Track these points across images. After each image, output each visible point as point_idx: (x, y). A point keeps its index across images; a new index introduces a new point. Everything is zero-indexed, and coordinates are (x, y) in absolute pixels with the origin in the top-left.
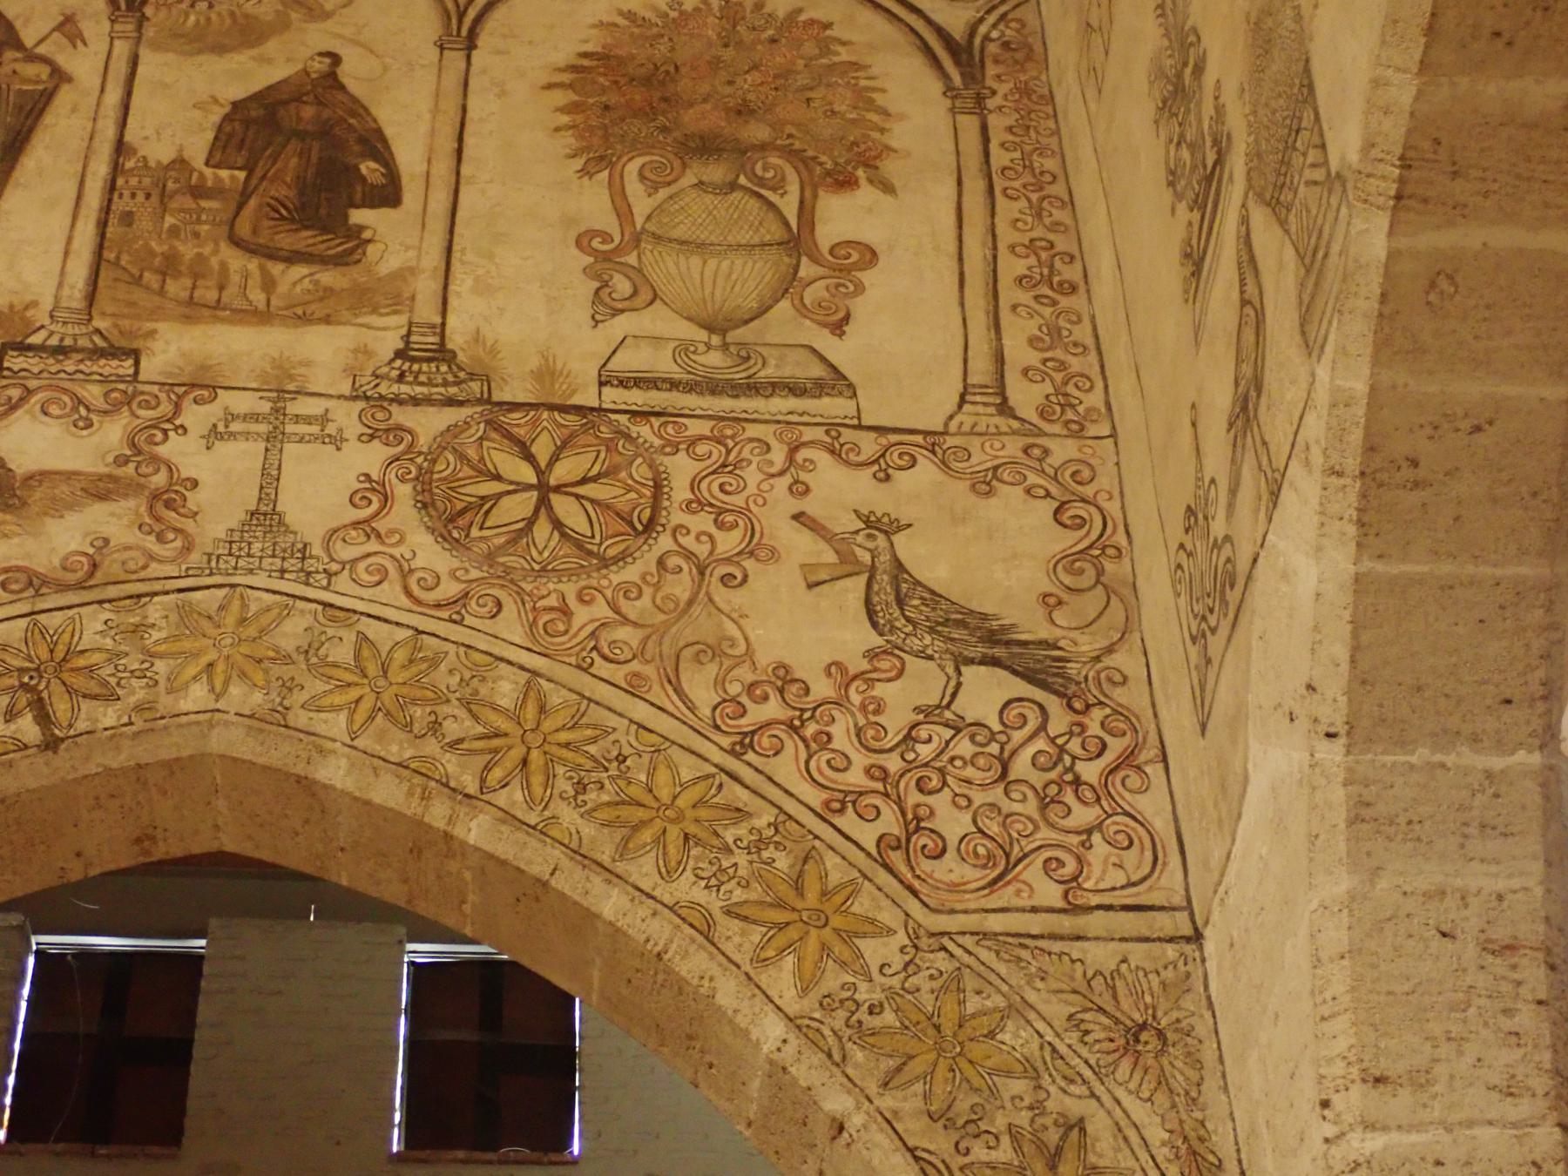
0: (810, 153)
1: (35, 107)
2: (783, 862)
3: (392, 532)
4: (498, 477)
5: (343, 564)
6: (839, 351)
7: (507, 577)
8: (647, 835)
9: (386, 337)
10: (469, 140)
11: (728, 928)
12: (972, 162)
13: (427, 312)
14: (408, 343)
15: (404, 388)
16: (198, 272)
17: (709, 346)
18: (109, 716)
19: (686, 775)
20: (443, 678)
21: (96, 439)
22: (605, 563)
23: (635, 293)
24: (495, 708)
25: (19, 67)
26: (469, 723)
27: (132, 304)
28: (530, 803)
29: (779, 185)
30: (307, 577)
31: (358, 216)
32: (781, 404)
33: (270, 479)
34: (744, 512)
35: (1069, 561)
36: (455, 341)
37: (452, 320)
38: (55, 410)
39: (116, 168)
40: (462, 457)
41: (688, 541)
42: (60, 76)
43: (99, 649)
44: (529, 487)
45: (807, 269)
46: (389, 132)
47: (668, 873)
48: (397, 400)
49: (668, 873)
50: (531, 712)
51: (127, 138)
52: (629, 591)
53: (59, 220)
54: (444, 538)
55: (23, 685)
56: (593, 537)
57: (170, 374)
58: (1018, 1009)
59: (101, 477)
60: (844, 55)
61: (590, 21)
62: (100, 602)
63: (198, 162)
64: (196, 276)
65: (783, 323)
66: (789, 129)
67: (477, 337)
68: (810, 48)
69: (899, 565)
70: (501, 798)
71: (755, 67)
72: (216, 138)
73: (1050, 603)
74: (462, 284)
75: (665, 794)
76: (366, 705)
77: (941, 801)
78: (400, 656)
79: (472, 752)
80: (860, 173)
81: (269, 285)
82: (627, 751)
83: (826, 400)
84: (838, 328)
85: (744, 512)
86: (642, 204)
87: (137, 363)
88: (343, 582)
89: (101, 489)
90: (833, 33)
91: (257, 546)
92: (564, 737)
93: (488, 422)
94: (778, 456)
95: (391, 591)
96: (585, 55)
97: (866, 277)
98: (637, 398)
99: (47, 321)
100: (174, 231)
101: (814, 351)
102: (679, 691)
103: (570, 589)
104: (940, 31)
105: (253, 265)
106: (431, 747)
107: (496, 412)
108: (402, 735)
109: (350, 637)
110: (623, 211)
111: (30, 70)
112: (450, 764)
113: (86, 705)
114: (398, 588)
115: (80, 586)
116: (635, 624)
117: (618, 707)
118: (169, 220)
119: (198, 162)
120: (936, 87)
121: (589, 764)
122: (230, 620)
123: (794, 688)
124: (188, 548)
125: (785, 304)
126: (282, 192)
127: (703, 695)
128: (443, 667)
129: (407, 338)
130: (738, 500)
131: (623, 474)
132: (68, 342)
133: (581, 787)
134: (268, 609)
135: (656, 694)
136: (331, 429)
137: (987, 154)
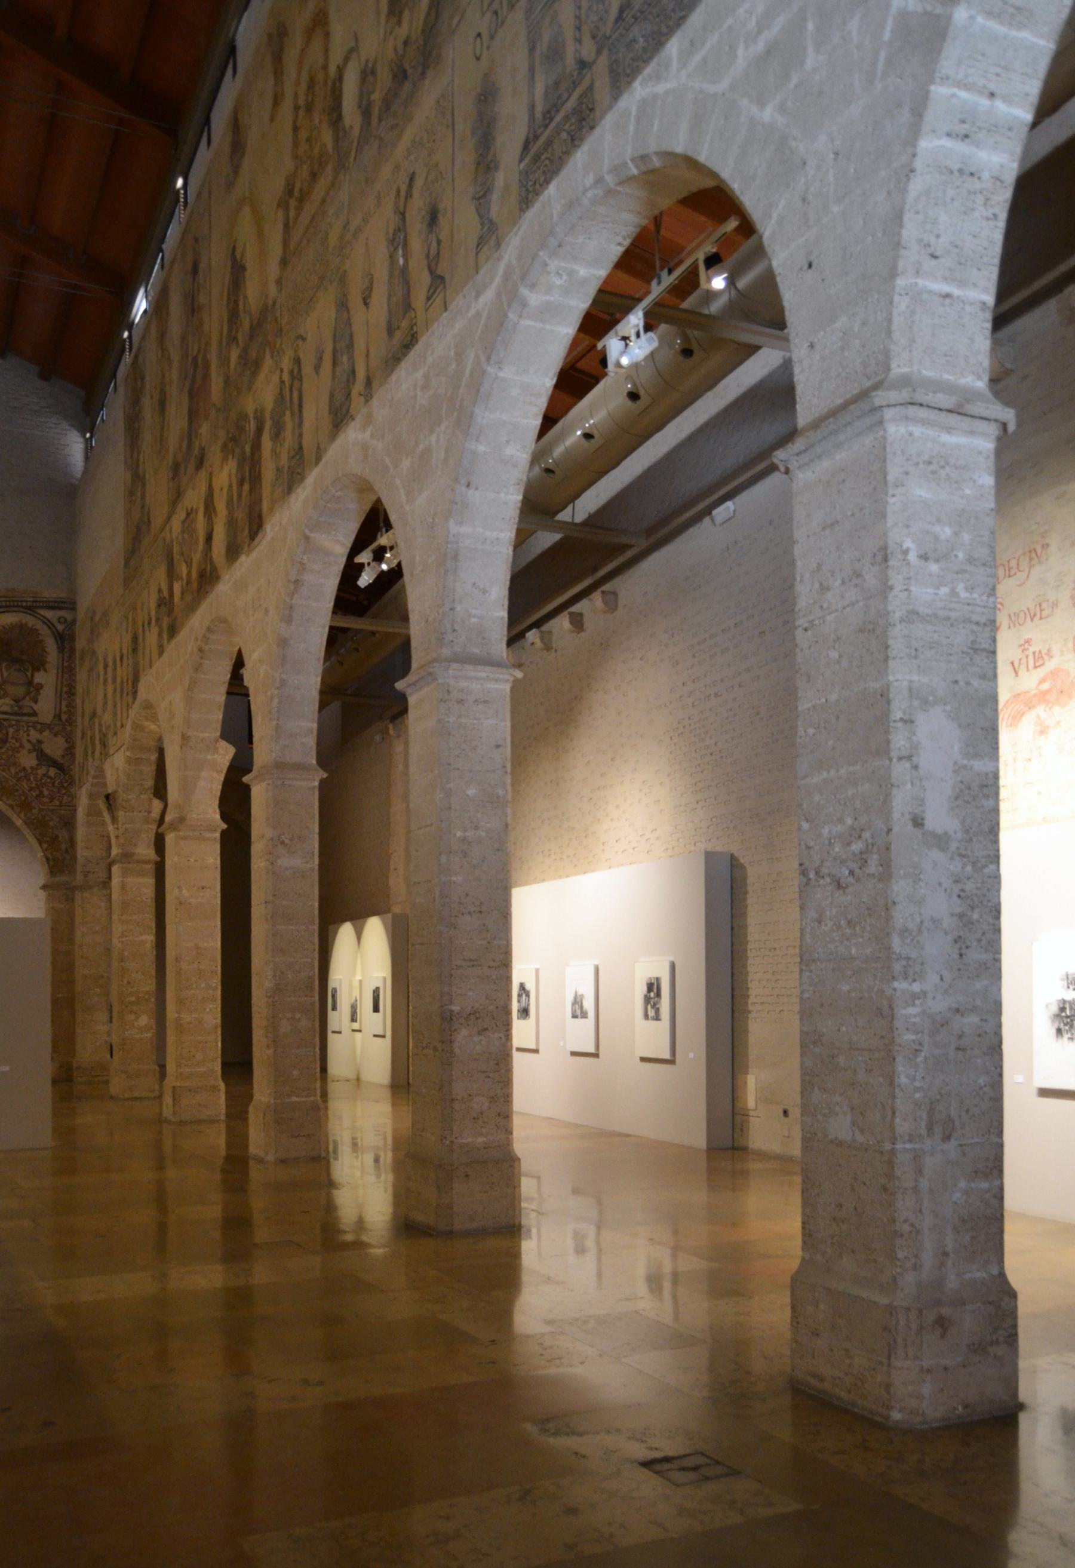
2: (23, 798)
6: (36, 707)
11: (15, 808)
19: (11, 784)
32: (26, 718)
35: (66, 750)
45: (32, 689)
47: (8, 799)
49: (8, 799)
58: (52, 820)
65: (27, 702)
69: (42, 751)
73: (63, 756)
77: (45, 789)
84: (36, 702)
97: (41, 691)
120: (55, 646)
125: (27, 698)
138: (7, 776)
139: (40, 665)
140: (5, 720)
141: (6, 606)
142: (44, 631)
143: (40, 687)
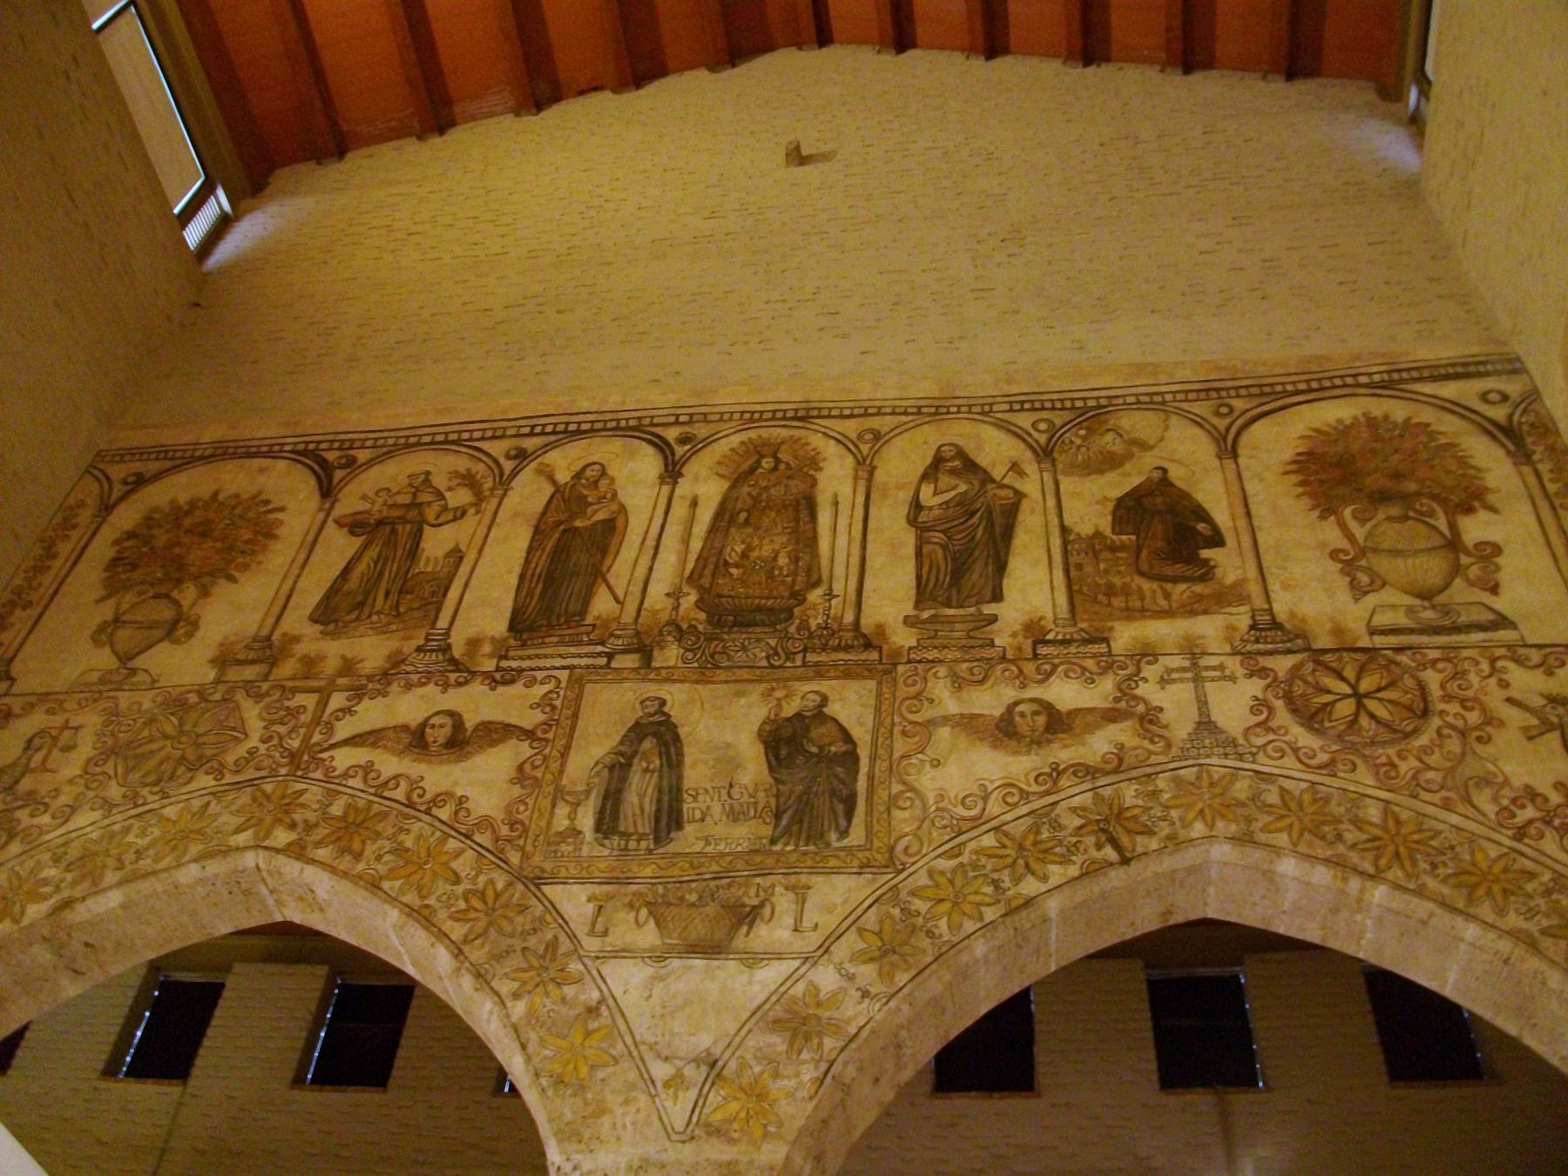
0: (1444, 495)
1: (1012, 511)
3: (1280, 728)
4: (1329, 692)
5: (1259, 747)
6: (1502, 604)
7: (1353, 748)
8: (1481, 891)
9: (1241, 618)
10: (1253, 507)
12: (1537, 492)
13: (1260, 603)
14: (1254, 621)
15: (1261, 646)
16: (1126, 591)
17: (1425, 608)
18: (1154, 844)
19: (1493, 852)
20: (1336, 809)
21: (1099, 688)
22: (1407, 736)
23: (1372, 582)
24: (1371, 824)
25: (996, 491)
26: (1358, 833)
27: (1097, 613)
28: (1408, 876)
29: (1432, 514)
30: (1240, 757)
31: (1205, 553)
32: (1477, 637)
33: (1202, 703)
34: (1476, 699)
36: (1282, 616)
37: (1276, 607)
38: (1072, 674)
39: (1065, 543)
40: (1306, 682)
41: (1450, 719)
42: (1020, 495)
43: (1136, 806)
44: (1348, 696)
45: (1464, 560)
46: (1206, 506)
47: (1501, 912)
48: (1260, 653)
49: (1501, 912)
50: (1391, 823)
51: (1066, 523)
52: (1426, 750)
53: (1042, 572)
54: (1310, 728)
55: (1102, 830)
56: (1330, 721)
57: (1128, 650)
59: (1110, 710)
60: (1443, 440)
61: (1296, 435)
62: (1129, 780)
63: (1108, 532)
64: (1127, 595)
65: (1460, 592)
66: (1428, 483)
67: (1292, 615)
68: (1424, 439)
70: (1390, 875)
71: (1396, 451)
72: (1114, 519)
74: (1274, 586)
75: (1484, 865)
76: (1297, 827)
78: (1307, 798)
79: (1364, 850)
80: (1476, 504)
81: (1167, 596)
82: (1454, 843)
83: (1501, 632)
84: (1494, 590)
85: (1476, 699)
86: (1360, 532)
87: (1109, 646)
88: (1261, 757)
89: (1111, 716)
90: (1429, 429)
91: (1207, 741)
92: (1416, 837)
93: (1314, 661)
94: (1485, 666)
95: (1290, 761)
96: (1299, 454)
97: (1499, 560)
98: (1393, 640)
99: (1053, 627)
100: (1106, 571)
101: (1484, 605)
102: (1474, 806)
103: (1392, 751)
104: (1491, 421)
105: (1155, 586)
106: (1341, 848)
107: (1316, 654)
108: (1321, 843)
109: (1274, 789)
110: (1350, 536)
111: (1003, 493)
112: (1354, 857)
113: (1139, 839)
114: (1293, 758)
115: (1115, 771)
116: (1436, 770)
117: (1441, 818)
118: (1102, 566)
119: (1108, 532)
120: (1500, 453)
121: (1434, 852)
122: (1205, 783)
123: (1539, 799)
124: (1169, 746)
125: (1458, 581)
126: (1159, 544)
127: (1490, 809)
128: (1333, 803)
129: (1253, 617)
130: (1470, 693)
131: (1400, 684)
132: (1068, 637)
133: (1434, 866)
134: (1224, 777)
135: (1460, 808)
136: (1227, 673)
137: (1543, 487)
138: (1472, 826)
139: (1472, 497)
140: (1399, 650)
141: (1311, 390)
142: (1448, 425)
143: (1490, 552)
